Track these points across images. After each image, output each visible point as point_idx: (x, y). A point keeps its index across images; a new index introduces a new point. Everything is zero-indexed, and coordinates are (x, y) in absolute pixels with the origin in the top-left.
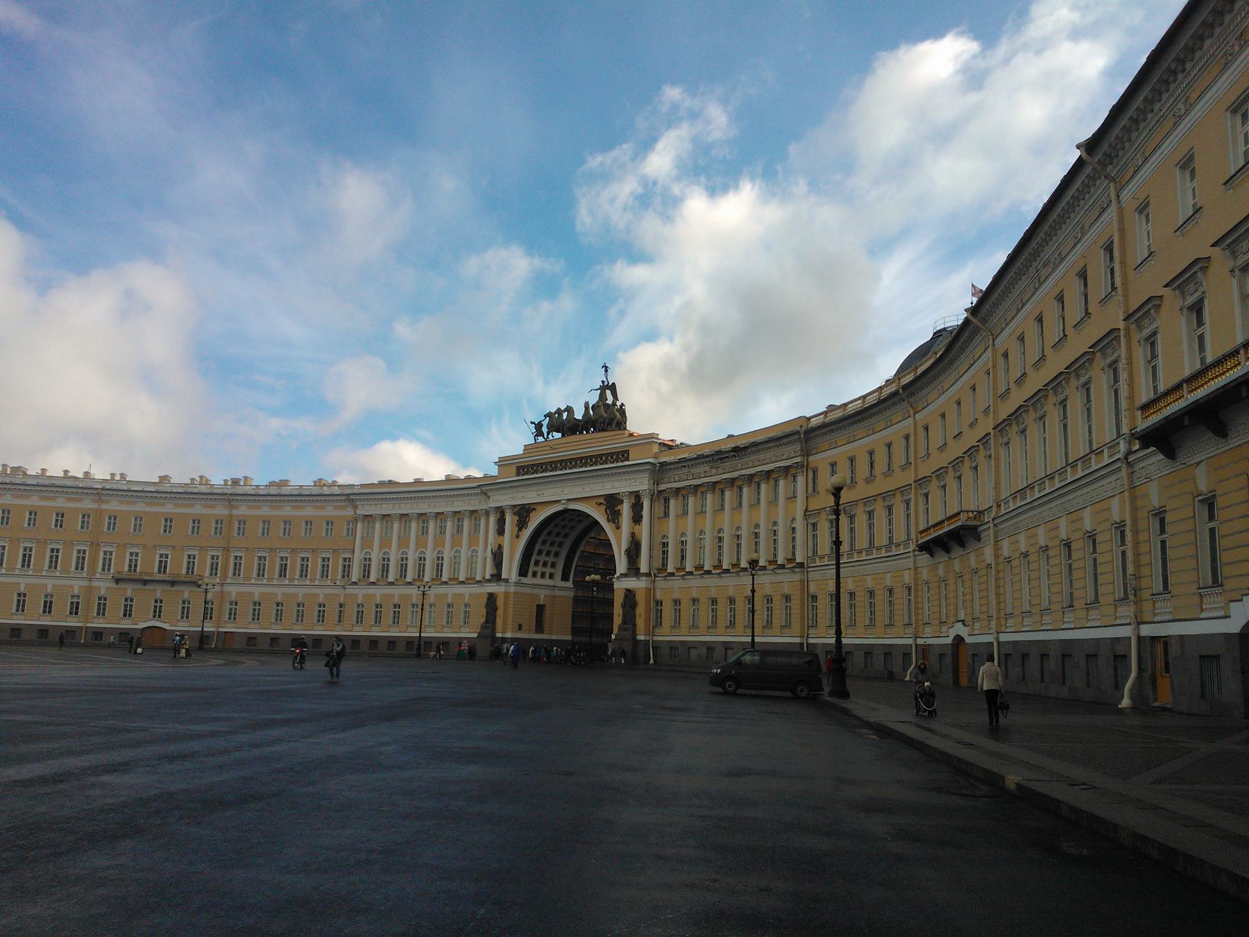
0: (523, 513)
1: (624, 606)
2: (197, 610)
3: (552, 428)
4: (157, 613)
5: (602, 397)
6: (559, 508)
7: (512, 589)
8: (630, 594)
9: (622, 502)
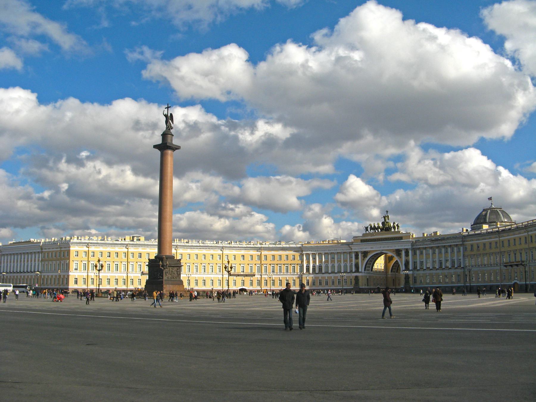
0: (365, 254)
1: (405, 278)
2: (255, 283)
3: (371, 228)
4: (243, 284)
5: (385, 220)
6: (379, 252)
7: (363, 274)
8: (407, 276)
9: (402, 251)
